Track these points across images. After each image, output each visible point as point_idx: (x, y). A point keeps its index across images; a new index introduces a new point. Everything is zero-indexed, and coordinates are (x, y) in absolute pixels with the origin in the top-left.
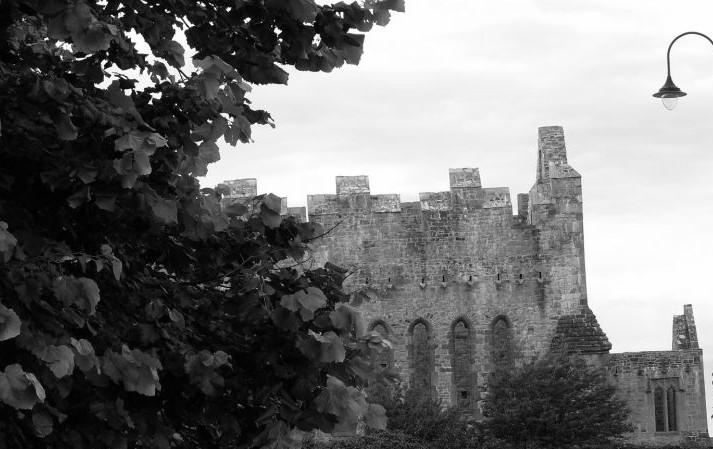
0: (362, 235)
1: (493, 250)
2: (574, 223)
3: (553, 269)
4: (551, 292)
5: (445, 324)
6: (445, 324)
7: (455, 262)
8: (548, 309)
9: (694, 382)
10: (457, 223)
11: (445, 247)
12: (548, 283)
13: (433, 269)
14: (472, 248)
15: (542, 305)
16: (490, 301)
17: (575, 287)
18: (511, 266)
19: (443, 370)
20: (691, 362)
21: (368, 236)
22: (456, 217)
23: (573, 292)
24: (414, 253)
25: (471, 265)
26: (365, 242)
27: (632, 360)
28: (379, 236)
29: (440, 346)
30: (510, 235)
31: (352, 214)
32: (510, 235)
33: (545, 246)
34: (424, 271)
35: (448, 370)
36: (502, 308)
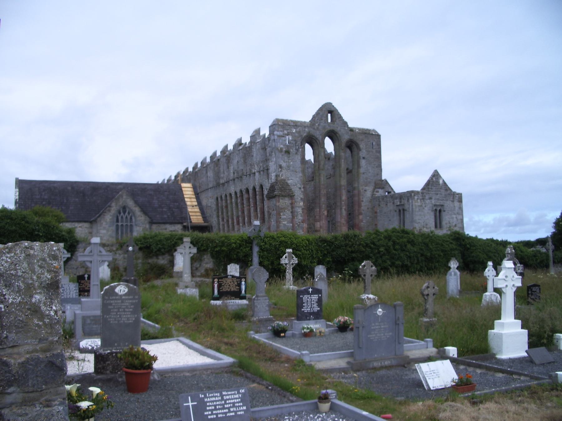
8: (270, 181)
9: (410, 206)
19: (252, 207)
23: (274, 172)
26: (237, 161)
33: (268, 155)
34: (247, 170)
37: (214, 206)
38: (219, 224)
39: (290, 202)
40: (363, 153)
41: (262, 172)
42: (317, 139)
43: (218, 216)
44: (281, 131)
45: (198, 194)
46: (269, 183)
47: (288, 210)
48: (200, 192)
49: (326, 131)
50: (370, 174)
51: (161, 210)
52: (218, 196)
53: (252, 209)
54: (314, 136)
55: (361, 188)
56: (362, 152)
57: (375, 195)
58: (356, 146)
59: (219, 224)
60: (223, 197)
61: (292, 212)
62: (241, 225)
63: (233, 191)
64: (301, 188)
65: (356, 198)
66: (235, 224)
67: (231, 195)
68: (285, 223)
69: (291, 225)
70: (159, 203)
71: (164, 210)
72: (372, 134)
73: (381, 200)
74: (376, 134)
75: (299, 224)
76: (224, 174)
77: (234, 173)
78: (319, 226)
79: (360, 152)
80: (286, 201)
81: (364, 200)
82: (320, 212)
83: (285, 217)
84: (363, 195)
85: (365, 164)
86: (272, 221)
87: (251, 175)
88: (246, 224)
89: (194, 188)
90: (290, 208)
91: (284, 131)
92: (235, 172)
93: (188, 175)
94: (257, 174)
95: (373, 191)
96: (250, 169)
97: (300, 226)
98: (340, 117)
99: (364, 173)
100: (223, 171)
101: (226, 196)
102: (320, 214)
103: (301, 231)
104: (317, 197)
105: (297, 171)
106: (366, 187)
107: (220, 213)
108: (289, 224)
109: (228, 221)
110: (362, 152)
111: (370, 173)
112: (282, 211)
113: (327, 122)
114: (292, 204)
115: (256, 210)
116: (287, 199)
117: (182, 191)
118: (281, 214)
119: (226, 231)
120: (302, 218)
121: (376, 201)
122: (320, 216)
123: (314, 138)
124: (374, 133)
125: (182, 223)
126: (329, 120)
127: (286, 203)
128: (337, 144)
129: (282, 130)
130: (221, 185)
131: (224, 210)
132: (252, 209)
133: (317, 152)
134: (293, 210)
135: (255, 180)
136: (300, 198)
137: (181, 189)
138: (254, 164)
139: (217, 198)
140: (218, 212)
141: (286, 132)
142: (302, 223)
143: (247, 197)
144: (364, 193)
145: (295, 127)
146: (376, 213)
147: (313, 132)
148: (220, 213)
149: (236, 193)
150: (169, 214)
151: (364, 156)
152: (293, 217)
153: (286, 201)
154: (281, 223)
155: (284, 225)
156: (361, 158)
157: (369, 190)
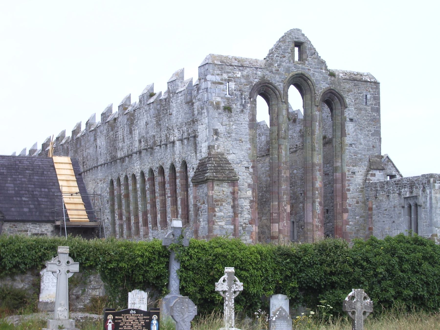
8: (198, 155)
9: (427, 198)
10: (169, 105)
15: (196, 152)
18: (186, 128)
19: (168, 197)
20: (425, 183)
23: (205, 141)
26: (146, 122)
27: (396, 184)
30: (185, 108)
31: (143, 107)
32: (185, 108)
33: (196, 112)
34: (161, 137)
36: (184, 155)
37: (106, 195)
38: (114, 224)
39: (231, 189)
40: (351, 112)
41: (185, 141)
42: (275, 88)
43: (113, 212)
44: (218, 75)
45: (80, 174)
46: (196, 159)
47: (227, 204)
48: (84, 172)
49: (291, 75)
50: (361, 147)
51: (18, 199)
52: (113, 179)
53: (169, 202)
54: (271, 84)
55: (346, 169)
56: (349, 110)
57: (369, 180)
58: (339, 100)
59: (114, 224)
60: (122, 179)
61: (233, 207)
62: (150, 226)
64: (248, 168)
65: (339, 186)
66: (140, 224)
68: (223, 223)
69: (232, 227)
70: (16, 189)
71: (24, 199)
72: (366, 81)
73: (379, 189)
74: (373, 80)
75: (244, 225)
76: (124, 143)
77: (140, 142)
78: (277, 230)
79: (346, 110)
80: (224, 189)
81: (351, 188)
82: (279, 206)
84: (349, 180)
85: (353, 129)
86: (201, 220)
87: (168, 146)
88: (159, 225)
89: (75, 164)
90: (230, 200)
91: (222, 75)
92: (142, 140)
93: (65, 143)
94: (178, 143)
95: (367, 175)
96: (166, 135)
97: (247, 229)
98: (314, 53)
99: (351, 145)
100: (122, 137)
102: (279, 209)
103: (248, 237)
104: (275, 182)
105: (243, 140)
106: (355, 168)
107: (116, 207)
108: (227, 226)
109: (129, 219)
110: (349, 110)
111: (361, 144)
112: (218, 205)
113: (292, 61)
114: (233, 193)
115: (175, 202)
116: (225, 185)
117: (55, 169)
118: (216, 209)
119: (125, 236)
120: (250, 217)
121: (371, 190)
122: (279, 214)
123: (271, 86)
124: (369, 80)
125: (53, 222)
126: (296, 58)
127: (224, 191)
128: (308, 96)
129: (219, 72)
130: (118, 161)
132: (169, 202)
133: (276, 110)
134: (236, 203)
135: (174, 153)
136: (246, 185)
137: (53, 166)
139: (112, 182)
140: (113, 205)
141: (225, 76)
142: (250, 224)
143: (160, 181)
144: (353, 177)
145: (241, 68)
146: (371, 209)
147: (269, 77)
148: (116, 207)
149: (142, 174)
150: (32, 206)
151: (351, 117)
152: (236, 214)
153: (224, 189)
154: (216, 224)
155: (221, 227)
156: (348, 119)
157: (360, 173)
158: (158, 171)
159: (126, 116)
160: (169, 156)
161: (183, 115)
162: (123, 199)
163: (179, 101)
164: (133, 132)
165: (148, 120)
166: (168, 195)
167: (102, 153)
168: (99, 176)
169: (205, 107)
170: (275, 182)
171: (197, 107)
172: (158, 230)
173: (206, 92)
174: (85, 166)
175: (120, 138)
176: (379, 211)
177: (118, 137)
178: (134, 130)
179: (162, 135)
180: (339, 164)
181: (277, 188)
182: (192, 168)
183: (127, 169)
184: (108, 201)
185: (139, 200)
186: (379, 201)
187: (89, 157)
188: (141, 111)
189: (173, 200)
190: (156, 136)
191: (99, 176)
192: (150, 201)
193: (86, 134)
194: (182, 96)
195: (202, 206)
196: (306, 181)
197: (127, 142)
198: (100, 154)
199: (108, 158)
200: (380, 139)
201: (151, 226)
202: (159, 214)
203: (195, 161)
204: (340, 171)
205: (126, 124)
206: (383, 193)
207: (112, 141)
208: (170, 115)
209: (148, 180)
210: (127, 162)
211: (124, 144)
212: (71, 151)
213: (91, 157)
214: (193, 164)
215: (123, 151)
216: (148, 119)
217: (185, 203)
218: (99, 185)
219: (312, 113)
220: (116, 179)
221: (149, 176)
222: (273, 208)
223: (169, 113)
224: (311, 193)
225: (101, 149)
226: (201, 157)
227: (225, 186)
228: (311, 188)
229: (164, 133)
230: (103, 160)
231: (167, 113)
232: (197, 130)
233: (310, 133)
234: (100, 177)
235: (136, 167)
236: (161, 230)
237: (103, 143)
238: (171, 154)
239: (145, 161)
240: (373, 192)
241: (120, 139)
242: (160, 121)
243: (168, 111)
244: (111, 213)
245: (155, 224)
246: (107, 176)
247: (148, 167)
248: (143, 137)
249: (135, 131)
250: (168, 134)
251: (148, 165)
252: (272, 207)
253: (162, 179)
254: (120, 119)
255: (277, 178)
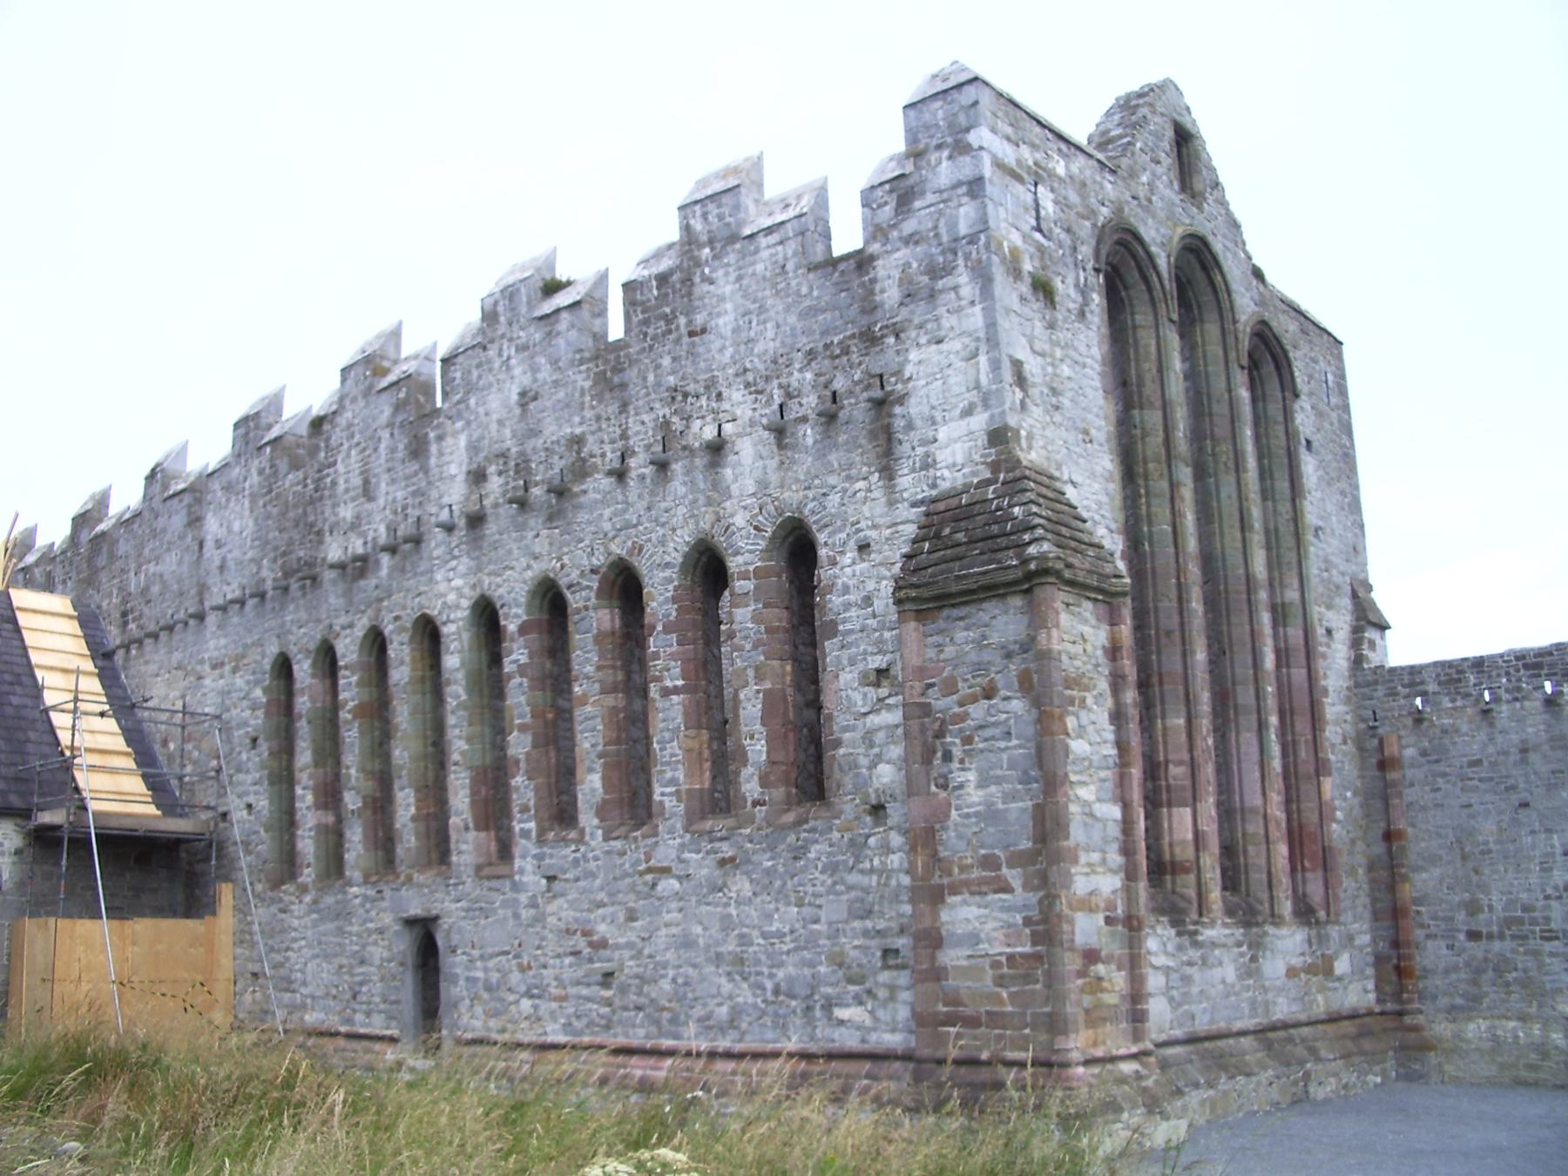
0: (520, 377)
1: (768, 344)
2: (962, 210)
3: (913, 355)
4: (910, 427)
5: (668, 565)
6: (668, 565)
7: (686, 395)
10: (690, 294)
11: (666, 362)
12: (902, 400)
13: (642, 430)
14: (722, 350)
16: (763, 484)
17: (973, 396)
18: (809, 376)
19: (666, 693)
21: (526, 380)
22: (688, 281)
23: (968, 412)
24: (607, 395)
25: (719, 395)
26: (523, 394)
27: (1526, 667)
28: (546, 374)
29: (660, 628)
31: (503, 336)
32: (804, 290)
33: (890, 294)
34: (624, 436)
35: (676, 691)
36: (791, 496)
37: (250, 717)
38: (287, 820)
43: (283, 779)
45: (108, 655)
46: (891, 503)
52: (293, 650)
58: (1278, 368)
60: (348, 649)
62: (524, 825)
63: (451, 598)
67: (429, 633)
77: (478, 477)
78: (1190, 836)
83: (1087, 747)
87: (677, 467)
88: (588, 819)
89: (89, 622)
92: (492, 469)
93: (37, 563)
96: (666, 424)
100: (357, 481)
101: (377, 642)
102: (1191, 749)
104: (1169, 633)
107: (304, 756)
109: (380, 806)
117: (18, 630)
119: (355, 874)
125: (25, 814)
130: (329, 575)
131: (352, 736)
137: (14, 621)
138: (710, 384)
139: (284, 667)
140: (286, 749)
143: (607, 626)
158: (595, 585)
159: (385, 396)
160: (682, 510)
161: (792, 319)
162: (347, 722)
163: (760, 267)
164: (434, 448)
165: (535, 380)
166: (669, 683)
167: (231, 564)
168: (207, 650)
169: (961, 262)
170: (1169, 633)
171: (896, 274)
172: (581, 840)
173: (965, 200)
174: (132, 626)
175: (341, 486)
176: (1442, 767)
177: (334, 483)
178: (440, 438)
179: (634, 427)
180: (1292, 595)
181: (1178, 658)
182: (852, 544)
183: (381, 600)
184: (254, 740)
185: (451, 720)
186: (1438, 731)
187: (155, 589)
188: (492, 353)
189: (698, 704)
190: (590, 439)
191: (207, 650)
192: (528, 719)
193: (146, 514)
194: (781, 243)
195: (977, 711)
196: (1231, 645)
197: (389, 492)
198: (222, 568)
199: (265, 573)
200: (1362, 527)
201: (532, 825)
202: (591, 770)
203: (880, 507)
204: (1300, 621)
205: (390, 425)
206: (1459, 703)
207: (295, 506)
208: (691, 334)
209: (523, 630)
210: (384, 572)
211: (368, 506)
212: (64, 582)
213: (165, 585)
214: (863, 525)
215: (363, 535)
216: (540, 376)
217: (785, 714)
218: (207, 682)
219: (1230, 391)
220: (312, 646)
221: (528, 613)
222: (1165, 743)
223: (683, 330)
224: (1252, 692)
225: (224, 550)
226: (934, 486)
227: (1088, 615)
228: (1251, 672)
229: (646, 418)
230: (235, 585)
231: (670, 332)
232: (898, 373)
233: (1231, 464)
234: (215, 654)
235: (442, 587)
236: (606, 838)
237: (236, 526)
238: (695, 501)
239: (510, 552)
240: (1402, 702)
241: (347, 491)
242: (621, 370)
243: (682, 320)
244: (271, 783)
245: (562, 814)
246: (259, 643)
247: (530, 573)
248: (504, 455)
249: (449, 441)
250: (675, 419)
251: (529, 567)
252: (1164, 735)
253: (612, 620)
254: (349, 415)
255: (1176, 619)
